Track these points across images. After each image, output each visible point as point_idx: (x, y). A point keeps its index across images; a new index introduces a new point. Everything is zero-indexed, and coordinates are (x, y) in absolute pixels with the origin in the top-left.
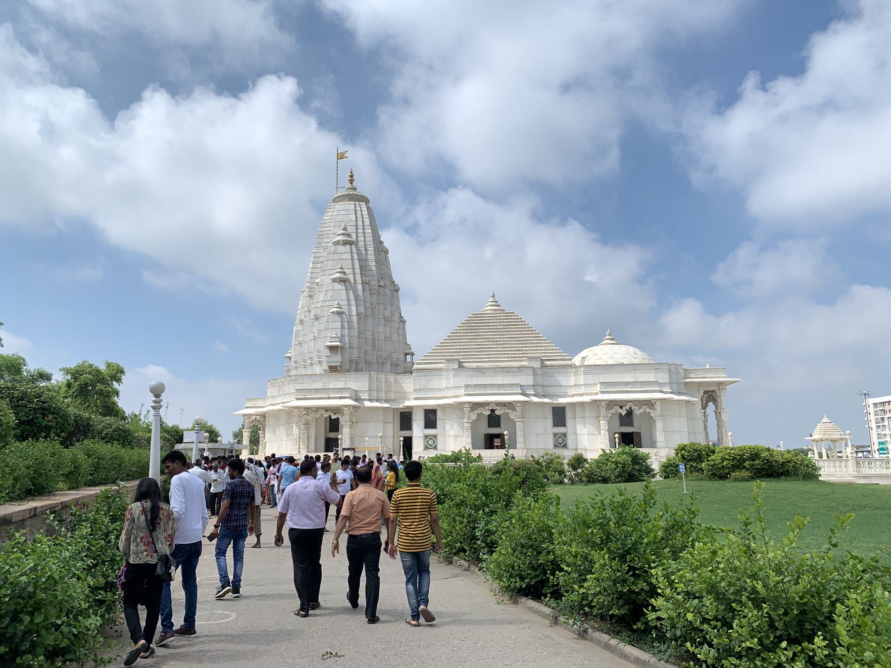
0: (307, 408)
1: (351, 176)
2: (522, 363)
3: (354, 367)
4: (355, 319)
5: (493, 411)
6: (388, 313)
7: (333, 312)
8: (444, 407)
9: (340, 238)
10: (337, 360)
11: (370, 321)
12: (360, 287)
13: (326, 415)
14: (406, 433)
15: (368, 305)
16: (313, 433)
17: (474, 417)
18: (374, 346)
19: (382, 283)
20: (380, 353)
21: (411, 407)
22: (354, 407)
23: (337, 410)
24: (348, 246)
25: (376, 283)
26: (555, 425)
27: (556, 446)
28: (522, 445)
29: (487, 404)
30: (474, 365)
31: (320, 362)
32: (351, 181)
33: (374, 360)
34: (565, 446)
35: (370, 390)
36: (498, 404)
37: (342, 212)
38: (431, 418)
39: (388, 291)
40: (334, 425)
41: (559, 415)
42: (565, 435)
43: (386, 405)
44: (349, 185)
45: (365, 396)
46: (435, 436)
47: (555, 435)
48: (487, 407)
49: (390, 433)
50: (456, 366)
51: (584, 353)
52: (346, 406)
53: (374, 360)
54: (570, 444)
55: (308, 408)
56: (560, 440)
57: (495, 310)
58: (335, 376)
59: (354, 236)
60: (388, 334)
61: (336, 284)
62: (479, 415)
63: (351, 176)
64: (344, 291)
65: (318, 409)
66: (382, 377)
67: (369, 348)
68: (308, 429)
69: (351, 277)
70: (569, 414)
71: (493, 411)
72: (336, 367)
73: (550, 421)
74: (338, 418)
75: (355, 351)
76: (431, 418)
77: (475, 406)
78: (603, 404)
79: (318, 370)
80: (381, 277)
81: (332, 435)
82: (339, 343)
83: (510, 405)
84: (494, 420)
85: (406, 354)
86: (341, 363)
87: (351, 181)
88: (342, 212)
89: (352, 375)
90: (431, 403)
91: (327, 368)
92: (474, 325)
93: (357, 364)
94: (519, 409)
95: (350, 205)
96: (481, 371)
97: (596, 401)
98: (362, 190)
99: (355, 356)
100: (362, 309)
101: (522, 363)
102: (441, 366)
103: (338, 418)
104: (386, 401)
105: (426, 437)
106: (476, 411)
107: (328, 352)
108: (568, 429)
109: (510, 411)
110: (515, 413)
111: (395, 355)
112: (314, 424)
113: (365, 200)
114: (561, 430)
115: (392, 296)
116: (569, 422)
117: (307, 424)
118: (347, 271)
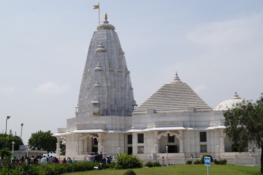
0: (83, 134)
1: (106, 16)
2: (185, 110)
3: (105, 113)
4: (106, 89)
5: (169, 134)
6: (123, 85)
7: (95, 86)
8: (146, 132)
9: (99, 49)
10: (96, 110)
11: (114, 90)
12: (108, 73)
13: (90, 137)
14: (129, 145)
15: (113, 82)
16: (86, 145)
17: (159, 137)
18: (116, 102)
19: (120, 70)
20: (118, 106)
21: (131, 133)
23: (96, 135)
24: (103, 53)
25: (117, 71)
26: (201, 141)
27: (201, 151)
28: (182, 151)
29: (165, 131)
30: (162, 112)
31: (89, 111)
32: (106, 18)
33: (116, 109)
34: (206, 151)
35: (112, 124)
36: (171, 131)
37: (101, 36)
38: (141, 138)
39: (124, 75)
40: (96, 142)
41: (203, 136)
42: (206, 146)
43: (120, 132)
45: (110, 127)
46: (143, 147)
47: (201, 146)
48: (166, 133)
49: (122, 145)
50: (153, 111)
51: (221, 104)
52: (99, 132)
53: (116, 109)
54: (208, 151)
55: (83, 133)
56: (204, 148)
57: (177, 82)
58: (95, 117)
59: (106, 47)
60: (123, 96)
61: (96, 72)
62: (163, 137)
63: (106, 16)
64: (100, 76)
65: (88, 133)
66: (118, 117)
67: (113, 103)
68: (83, 143)
69: (104, 68)
70: (208, 135)
71: (169, 134)
72: (96, 113)
73: (198, 139)
74: (96, 139)
75: (106, 105)
76: (141, 138)
77: (160, 132)
78: (222, 130)
79: (88, 114)
80: (120, 67)
81: (95, 146)
82: (97, 102)
83: (176, 131)
84: (171, 139)
85: (134, 106)
86: (99, 111)
87: (106, 18)
88: (101, 36)
89: (104, 117)
90: (140, 131)
91: (92, 113)
92: (165, 91)
93: (107, 111)
94: (181, 133)
95: (105, 32)
96: (164, 115)
97: (218, 129)
98: (111, 23)
99: (106, 108)
100: (109, 84)
101: (185, 110)
102: (146, 112)
103: (96, 139)
104: (120, 130)
105: (139, 147)
106: (160, 135)
107: (92, 106)
108: (207, 143)
109: (176, 134)
110: (179, 135)
111: (127, 107)
112: (86, 141)
113: (112, 28)
114: (204, 143)
115: (126, 76)
116: (208, 139)
117: (83, 141)
118: (102, 65)
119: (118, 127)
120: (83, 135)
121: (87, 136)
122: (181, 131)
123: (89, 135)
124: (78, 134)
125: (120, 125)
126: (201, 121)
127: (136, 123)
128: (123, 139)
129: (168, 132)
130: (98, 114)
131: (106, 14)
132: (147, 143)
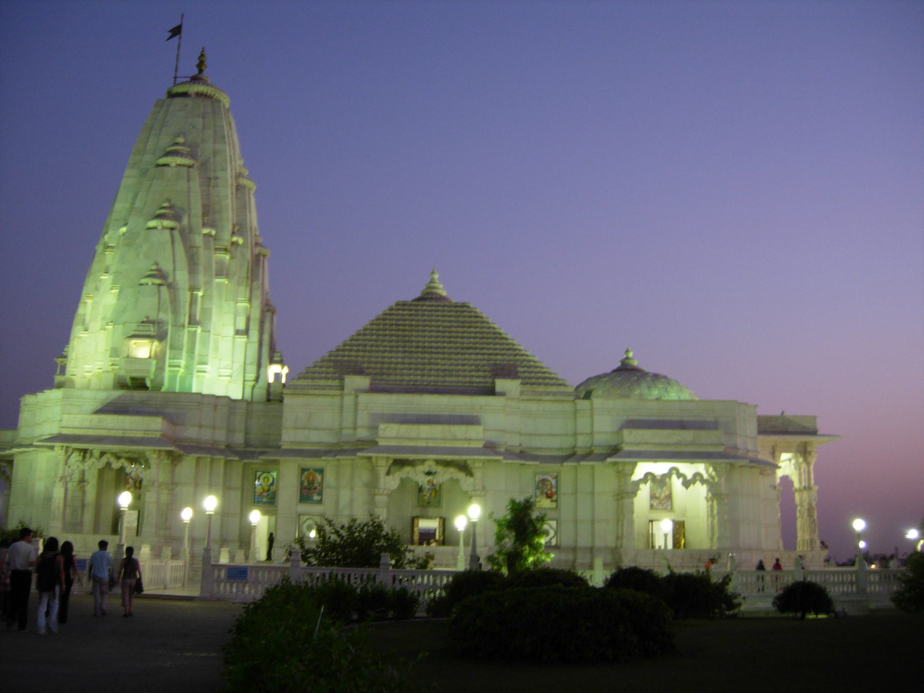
13: (116, 465)
22: (169, 453)
44: (195, 71)
109: (461, 475)
110: (470, 480)
119: (221, 436)
120: (84, 457)
121: (104, 459)
122: (480, 465)
123: (112, 460)
124: (66, 452)
125: (230, 431)
126: (541, 435)
127: (297, 428)
128: (239, 484)
129: (430, 466)
130: (148, 383)
131: (202, 55)
132: (337, 502)
